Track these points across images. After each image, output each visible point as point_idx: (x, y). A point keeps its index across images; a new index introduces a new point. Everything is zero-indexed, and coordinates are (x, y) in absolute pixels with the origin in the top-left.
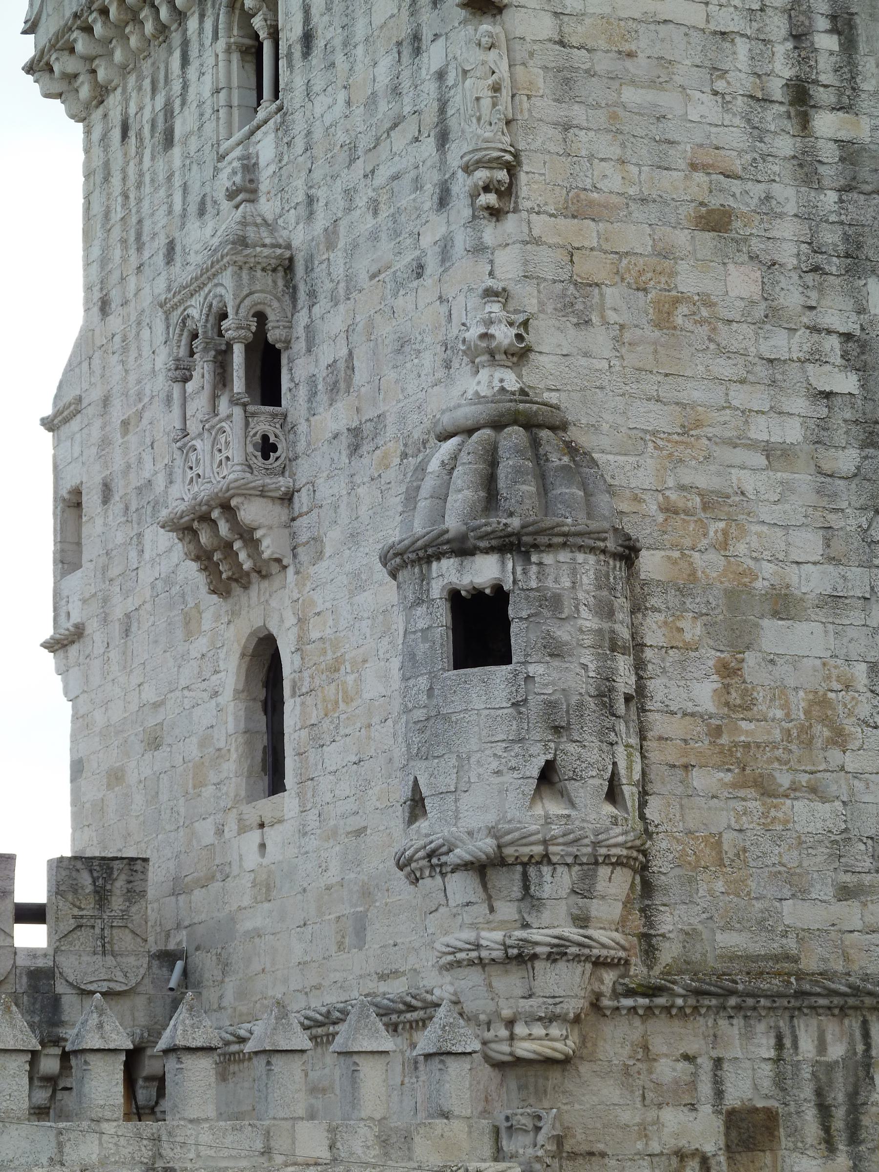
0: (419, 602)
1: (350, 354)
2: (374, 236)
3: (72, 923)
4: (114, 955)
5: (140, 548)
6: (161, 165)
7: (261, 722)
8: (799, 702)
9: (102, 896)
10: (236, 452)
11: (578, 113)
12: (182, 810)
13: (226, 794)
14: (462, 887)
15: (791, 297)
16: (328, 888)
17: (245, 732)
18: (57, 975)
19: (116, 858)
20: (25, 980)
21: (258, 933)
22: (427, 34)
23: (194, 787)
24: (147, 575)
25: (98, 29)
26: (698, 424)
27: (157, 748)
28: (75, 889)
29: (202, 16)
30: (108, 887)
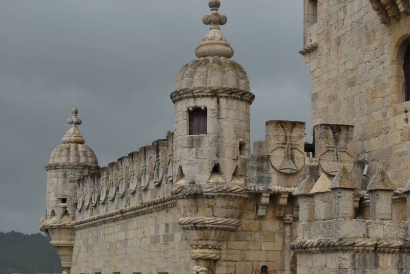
3: (326, 149)
4: (341, 162)
5: (345, 11)
7: (402, 73)
9: (336, 140)
12: (366, 109)
13: (388, 100)
17: (396, 77)
18: (320, 168)
19: (342, 125)
20: (308, 170)
21: (404, 153)
23: (372, 99)
24: (348, 21)
27: (353, 86)
30: (339, 136)
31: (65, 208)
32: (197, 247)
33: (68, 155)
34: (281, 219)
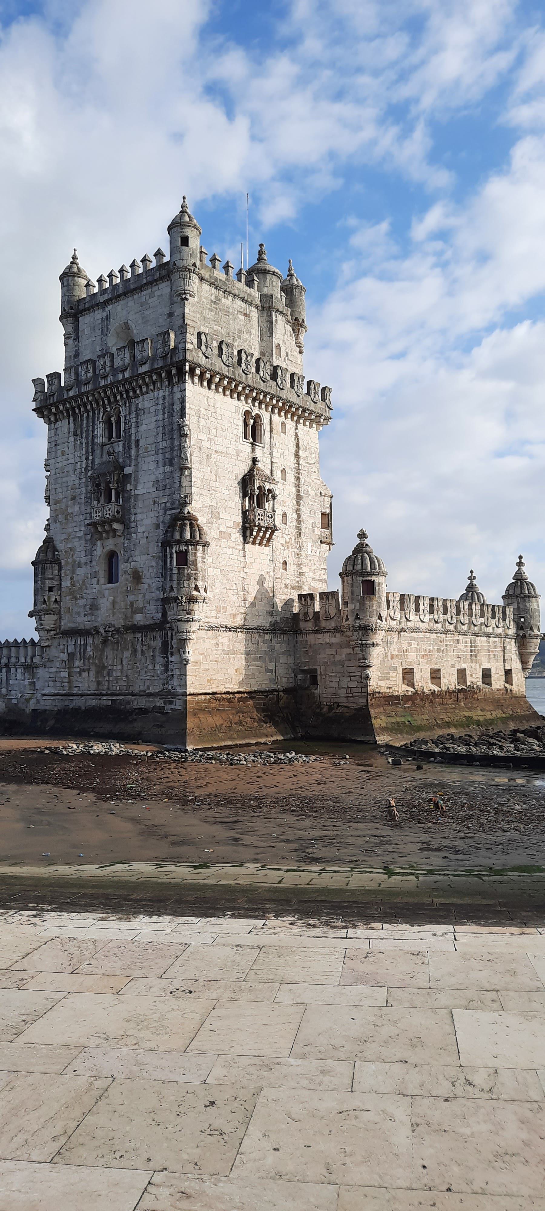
11: (57, 486)
15: (83, 508)
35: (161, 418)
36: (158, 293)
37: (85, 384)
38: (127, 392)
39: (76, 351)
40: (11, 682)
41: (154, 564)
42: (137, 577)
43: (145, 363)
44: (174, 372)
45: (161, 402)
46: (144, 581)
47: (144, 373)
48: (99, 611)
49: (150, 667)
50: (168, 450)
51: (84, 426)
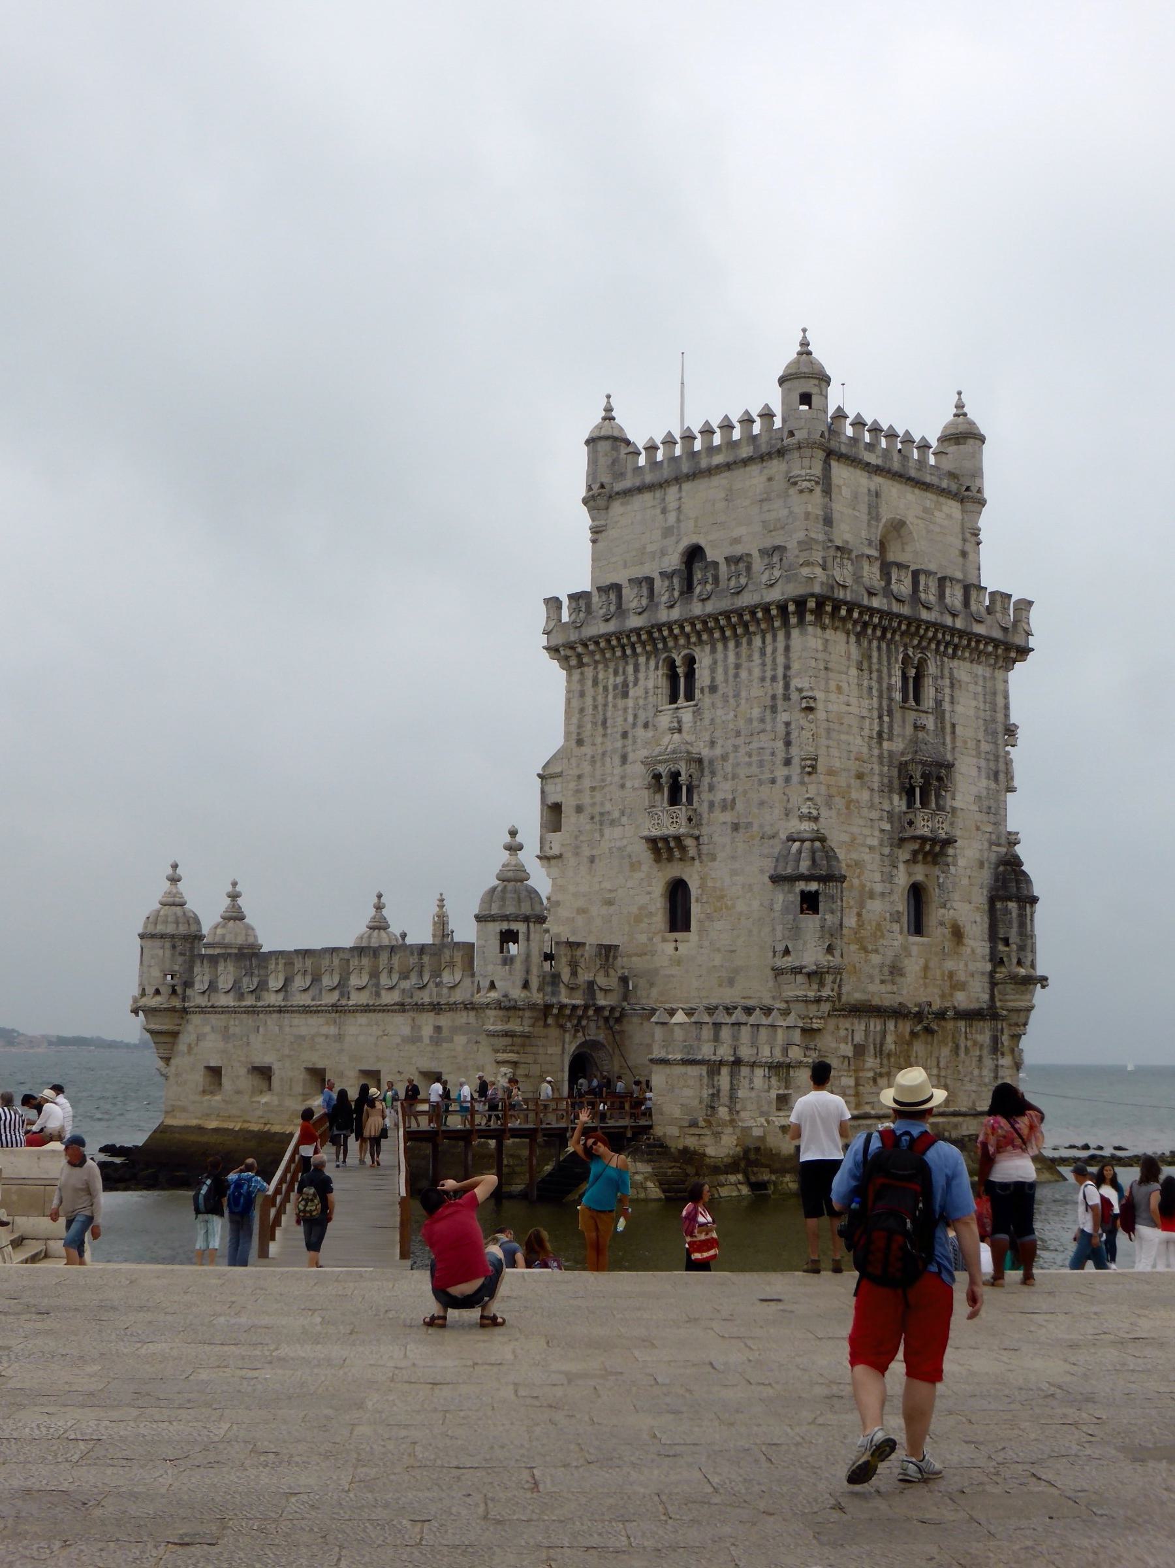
0: (790, 892)
1: (734, 799)
2: (750, 764)
6: (621, 703)
8: (874, 924)
9: (607, 957)
10: (684, 821)
11: (831, 743)
14: (800, 979)
15: (877, 800)
16: (714, 967)
21: (673, 976)
22: (780, 708)
25: (592, 647)
26: (854, 840)
28: (601, 954)
29: (648, 659)
31: (173, 986)
32: (504, 1051)
33: (177, 923)
34: (562, 1026)
35: (982, 706)
36: (945, 508)
37: (898, 600)
38: (947, 644)
39: (826, 513)
40: (740, 1094)
41: (978, 919)
42: (957, 934)
43: (980, 622)
44: (1013, 655)
45: (981, 683)
46: (966, 941)
47: (985, 637)
48: (903, 979)
49: (976, 1072)
50: (992, 757)
51: (875, 660)
